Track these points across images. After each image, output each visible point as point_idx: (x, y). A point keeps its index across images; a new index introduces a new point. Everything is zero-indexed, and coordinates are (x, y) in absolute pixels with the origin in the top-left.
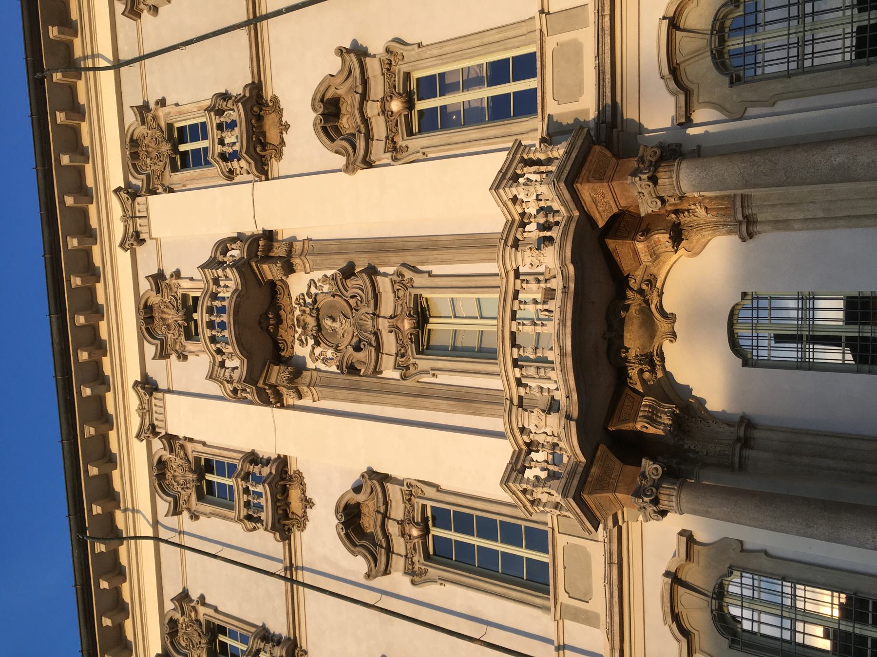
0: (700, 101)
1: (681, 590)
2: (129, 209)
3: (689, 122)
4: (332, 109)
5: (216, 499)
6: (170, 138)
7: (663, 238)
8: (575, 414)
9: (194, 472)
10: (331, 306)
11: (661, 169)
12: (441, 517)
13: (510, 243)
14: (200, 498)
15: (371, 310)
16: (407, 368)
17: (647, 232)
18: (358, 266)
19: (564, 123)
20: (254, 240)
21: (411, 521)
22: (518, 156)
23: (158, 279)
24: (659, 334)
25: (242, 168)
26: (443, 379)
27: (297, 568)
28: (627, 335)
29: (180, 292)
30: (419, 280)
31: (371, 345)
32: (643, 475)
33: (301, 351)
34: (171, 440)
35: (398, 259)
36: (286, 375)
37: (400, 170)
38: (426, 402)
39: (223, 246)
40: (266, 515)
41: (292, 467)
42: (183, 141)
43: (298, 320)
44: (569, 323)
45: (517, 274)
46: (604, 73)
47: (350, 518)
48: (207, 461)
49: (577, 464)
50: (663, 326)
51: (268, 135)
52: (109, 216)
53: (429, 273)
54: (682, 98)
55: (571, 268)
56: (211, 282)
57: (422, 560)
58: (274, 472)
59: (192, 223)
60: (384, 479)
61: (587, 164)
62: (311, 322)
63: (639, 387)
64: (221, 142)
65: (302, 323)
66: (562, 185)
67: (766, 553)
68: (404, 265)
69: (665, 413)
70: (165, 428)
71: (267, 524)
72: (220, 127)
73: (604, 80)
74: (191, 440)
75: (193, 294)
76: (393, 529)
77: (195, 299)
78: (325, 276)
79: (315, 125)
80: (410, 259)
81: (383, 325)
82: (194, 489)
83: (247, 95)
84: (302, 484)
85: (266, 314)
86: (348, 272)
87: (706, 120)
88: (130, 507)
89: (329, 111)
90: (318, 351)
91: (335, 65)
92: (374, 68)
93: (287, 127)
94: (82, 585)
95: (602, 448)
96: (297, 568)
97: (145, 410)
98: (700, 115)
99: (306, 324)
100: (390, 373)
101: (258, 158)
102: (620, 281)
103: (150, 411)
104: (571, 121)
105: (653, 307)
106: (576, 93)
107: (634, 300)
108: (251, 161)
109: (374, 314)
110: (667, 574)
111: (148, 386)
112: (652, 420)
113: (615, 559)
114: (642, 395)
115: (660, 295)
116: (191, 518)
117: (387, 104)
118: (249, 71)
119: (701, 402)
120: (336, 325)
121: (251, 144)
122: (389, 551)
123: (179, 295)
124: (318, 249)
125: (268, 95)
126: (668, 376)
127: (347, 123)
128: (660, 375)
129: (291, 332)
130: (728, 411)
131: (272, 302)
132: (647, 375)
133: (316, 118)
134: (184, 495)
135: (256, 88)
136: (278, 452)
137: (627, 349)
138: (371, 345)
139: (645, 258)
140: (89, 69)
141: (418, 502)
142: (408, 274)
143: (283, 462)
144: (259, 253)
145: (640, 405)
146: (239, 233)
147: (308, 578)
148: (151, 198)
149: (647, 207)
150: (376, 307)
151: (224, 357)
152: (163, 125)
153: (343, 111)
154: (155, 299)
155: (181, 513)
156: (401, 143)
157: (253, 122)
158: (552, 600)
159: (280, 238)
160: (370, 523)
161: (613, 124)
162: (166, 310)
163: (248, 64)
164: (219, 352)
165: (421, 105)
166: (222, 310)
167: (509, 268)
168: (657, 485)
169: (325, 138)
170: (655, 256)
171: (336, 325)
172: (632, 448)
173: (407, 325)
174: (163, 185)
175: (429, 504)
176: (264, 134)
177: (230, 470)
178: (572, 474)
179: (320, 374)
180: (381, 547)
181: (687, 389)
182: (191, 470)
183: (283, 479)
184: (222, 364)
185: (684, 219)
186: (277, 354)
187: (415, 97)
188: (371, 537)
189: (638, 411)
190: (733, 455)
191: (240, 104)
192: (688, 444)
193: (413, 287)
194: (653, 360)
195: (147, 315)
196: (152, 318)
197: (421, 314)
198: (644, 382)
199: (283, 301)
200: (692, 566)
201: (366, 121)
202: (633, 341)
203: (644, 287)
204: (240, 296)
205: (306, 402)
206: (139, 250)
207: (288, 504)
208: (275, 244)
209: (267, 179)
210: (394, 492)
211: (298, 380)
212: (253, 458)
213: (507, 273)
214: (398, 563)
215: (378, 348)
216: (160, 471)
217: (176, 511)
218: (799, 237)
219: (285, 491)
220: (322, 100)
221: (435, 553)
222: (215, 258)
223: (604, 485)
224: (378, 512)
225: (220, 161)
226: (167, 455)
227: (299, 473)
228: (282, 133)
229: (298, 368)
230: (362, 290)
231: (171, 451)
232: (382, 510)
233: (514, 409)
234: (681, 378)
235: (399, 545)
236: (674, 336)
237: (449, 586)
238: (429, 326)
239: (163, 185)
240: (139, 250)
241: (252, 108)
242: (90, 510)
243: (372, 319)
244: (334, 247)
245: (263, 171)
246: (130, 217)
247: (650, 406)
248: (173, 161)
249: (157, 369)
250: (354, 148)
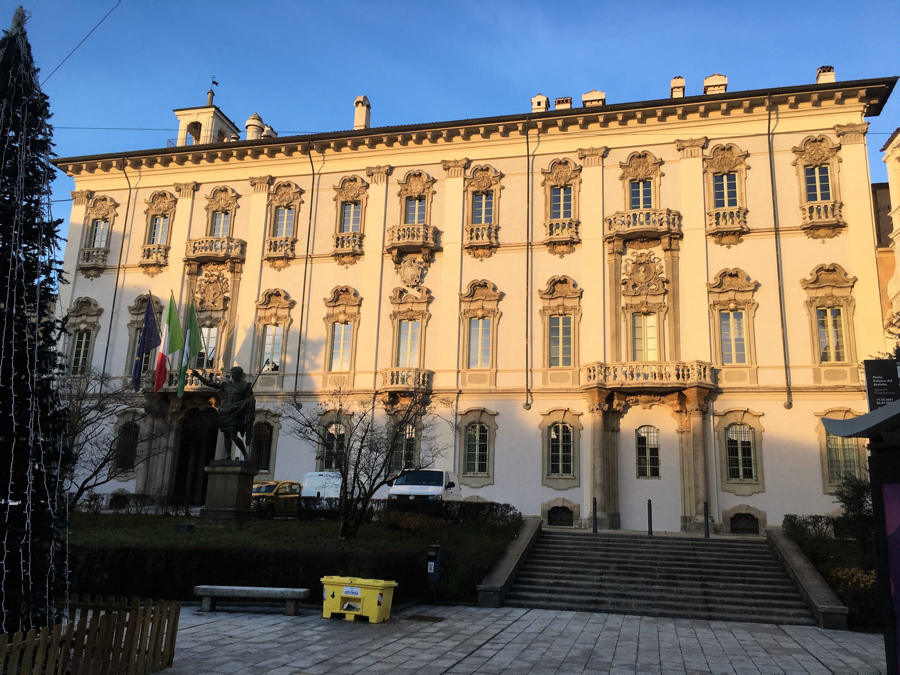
3: (714, 415)
7: (678, 408)
10: (650, 270)
12: (567, 322)
17: (680, 404)
18: (669, 286)
26: (623, 324)
30: (662, 314)
33: (629, 251)
35: (671, 305)
37: (706, 307)
80: (671, 310)
87: (714, 422)
92: (747, 296)
97: (593, 151)
106: (729, 379)
112: (618, 405)
120: (641, 273)
124: (674, 265)
125: (743, 237)
139: (671, 402)
140: (770, 114)
141: (572, 312)
142: (665, 310)
149: (689, 407)
152: (736, 168)
156: (718, 307)
170: (672, 405)
171: (641, 273)
172: (609, 399)
173: (644, 309)
185: (684, 414)
186: (628, 239)
194: (636, 402)
199: (652, 243)
205: (607, 256)
214: (546, 303)
218: (677, 446)
223: (600, 393)
244: (675, 273)
246: (693, 143)
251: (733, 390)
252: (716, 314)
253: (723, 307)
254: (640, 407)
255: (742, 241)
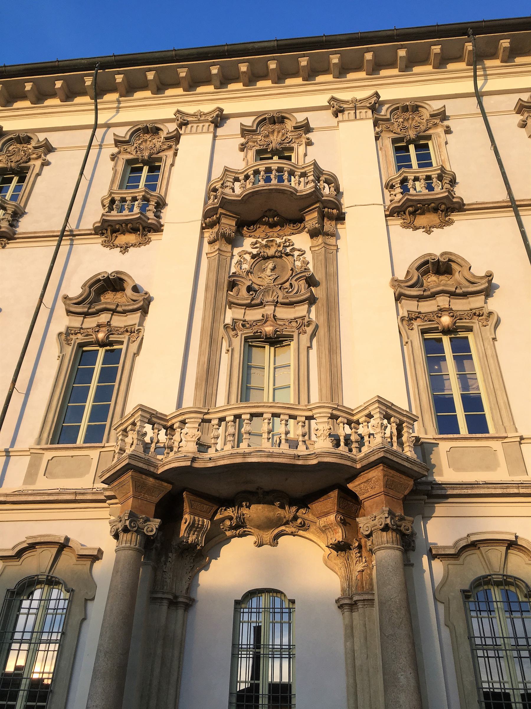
0: (450, 566)
1: (54, 550)
2: (362, 105)
3: (432, 557)
4: (443, 269)
5: (128, 175)
6: (419, 137)
7: (338, 536)
8: (196, 465)
9: (149, 157)
10: (283, 268)
11: (394, 534)
12: (113, 356)
13: (335, 412)
14: (129, 162)
15: (280, 300)
16: (234, 329)
17: (344, 523)
19: (431, 456)
20: (337, 206)
21: (110, 333)
22: (405, 419)
23: (306, 128)
24: (261, 533)
25: (395, 195)
26: (225, 358)
27: (72, 240)
28: (260, 507)
29: (295, 146)
30: (305, 339)
31: (253, 299)
32: (147, 520)
33: (247, 243)
34: (176, 138)
35: (322, 321)
36: (228, 232)
37: (393, 323)
38: (206, 344)
39: (332, 180)
40: (115, 216)
41: (153, 236)
42: (417, 148)
43: (272, 241)
44: (270, 460)
45: (309, 418)
46: (472, 488)
47: (113, 283)
48: (159, 168)
49: (156, 467)
50: (268, 536)
51: (422, 217)
52: (356, 88)
53: (310, 347)
54: (452, 551)
55: (315, 462)
56: (303, 171)
57: (78, 341)
58: (150, 221)
59: (350, 155)
60: (144, 310)
61: (399, 474)
62: (271, 252)
63: (218, 517)
64: (416, 179)
65: (270, 244)
66: (381, 455)
67: (84, 619)
68: (317, 327)
69: (197, 538)
70: (185, 134)
71: (107, 216)
72: (428, 178)
73: (466, 488)
74: (175, 154)
75: (293, 156)
76: (104, 318)
77: (289, 158)
78: (308, 263)
79: (430, 254)
80: (322, 332)
81: (269, 310)
82: (136, 157)
83: (455, 200)
84: (140, 244)
85: (278, 215)
86: (311, 282)
88: (121, 105)
89: (442, 266)
90: (248, 257)
91: (479, 270)
92: (476, 302)
93: (429, 232)
94: (58, 67)
95: (169, 487)
96: (72, 240)
97: (199, 117)
98: (438, 566)
99: (269, 247)
100: (230, 315)
101: (403, 209)
102: (304, 501)
103: (199, 121)
104: (433, 462)
105: (283, 528)
107: (288, 512)
108: (401, 203)
109: (277, 302)
110: (67, 539)
111: (219, 119)
112: (192, 527)
113: (79, 497)
114: (212, 519)
115: (293, 534)
116: (113, 155)
117: (447, 313)
118: (474, 201)
119: (206, 567)
121: (415, 203)
122: (86, 315)
123: (293, 145)
124: (329, 258)
125: (454, 217)
126: (228, 540)
127: (432, 281)
128: (228, 533)
129: (263, 235)
130: (199, 589)
131: (287, 219)
132: (228, 523)
133: (435, 255)
134: (131, 149)
135: (460, 207)
136: (165, 225)
137: (249, 507)
138: (253, 299)
139: (322, 522)
140: (475, 72)
141: (125, 338)
142: (309, 330)
143: (158, 229)
144: (326, 210)
145: (204, 517)
146: (343, 193)
147: (64, 249)
148: (371, 122)
149: (364, 523)
150: (282, 304)
151: (242, 181)
152: (430, 132)
153: (441, 278)
154: (289, 125)
155: (116, 146)
156: (416, 324)
157: (433, 205)
158: (46, 446)
159: (339, 226)
160: (109, 299)
161: (430, 496)
162: (281, 134)
163: (480, 200)
164: (247, 177)
165: (446, 341)
166: (280, 180)
167: (315, 411)
168: (139, 531)
169: (419, 263)
170: (324, 530)
171: (268, 272)
172: (169, 511)
173: (268, 329)
174: (381, 132)
175: (124, 347)
176: (423, 213)
177: (151, 187)
178: (148, 462)
179: (229, 258)
180: (89, 309)
181: (216, 556)
182: (151, 154)
183: (144, 228)
184: (237, 180)
185: (354, 553)
186: (244, 224)
187: (453, 336)
188: (96, 300)
189: (199, 516)
190: (164, 593)
191: (447, 194)
192: (172, 556)
193: (299, 334)
194: (240, 528)
195: (277, 119)
196: (274, 123)
197: (277, 341)
198: (222, 520)
199: (288, 229)
200: (74, 559)
201: (433, 296)
202: (255, 512)
203: (299, 521)
204: (292, 194)
205: (206, 248)
206: (329, 112)
207: (123, 233)
208: (333, 223)
209: (386, 216)
210: (134, 319)
211: (224, 241)
212: (161, 205)
213: (310, 410)
214: (76, 322)
215: (250, 306)
216: (151, 129)
217: (118, 142)
218: (340, 646)
219: (134, 230)
220: (450, 260)
221: (83, 351)
222: (323, 174)
223: (139, 488)
224: (117, 306)
225: (401, 178)
226: (163, 135)
227: (148, 242)
228: (423, 228)
229: (233, 241)
230: (297, 293)
231: (166, 139)
232: (119, 309)
233: (201, 416)
234: (226, 551)
235: (91, 322)
236: (260, 545)
237: (58, 363)
238: (267, 347)
239: (381, 132)
240: (329, 112)
241: (443, 203)
242: (119, 73)
243: (274, 301)
244: (331, 270)
245: (393, 213)
246: (356, 105)
247: (203, 525)
248: (401, 140)
249: (232, 127)
250: (412, 286)
251: (469, 493)
252: (416, 337)
253: (428, 325)
254: (250, 540)
255: (450, 223)
